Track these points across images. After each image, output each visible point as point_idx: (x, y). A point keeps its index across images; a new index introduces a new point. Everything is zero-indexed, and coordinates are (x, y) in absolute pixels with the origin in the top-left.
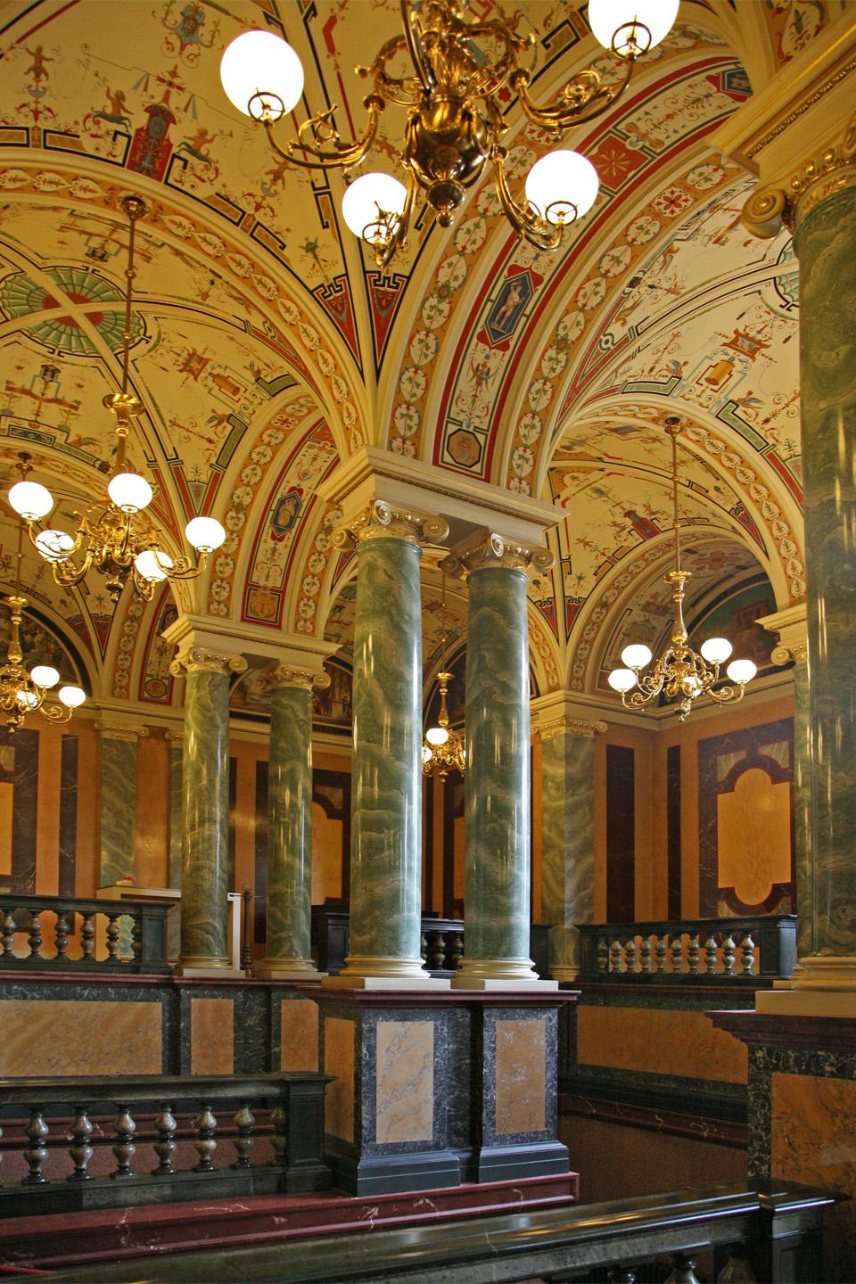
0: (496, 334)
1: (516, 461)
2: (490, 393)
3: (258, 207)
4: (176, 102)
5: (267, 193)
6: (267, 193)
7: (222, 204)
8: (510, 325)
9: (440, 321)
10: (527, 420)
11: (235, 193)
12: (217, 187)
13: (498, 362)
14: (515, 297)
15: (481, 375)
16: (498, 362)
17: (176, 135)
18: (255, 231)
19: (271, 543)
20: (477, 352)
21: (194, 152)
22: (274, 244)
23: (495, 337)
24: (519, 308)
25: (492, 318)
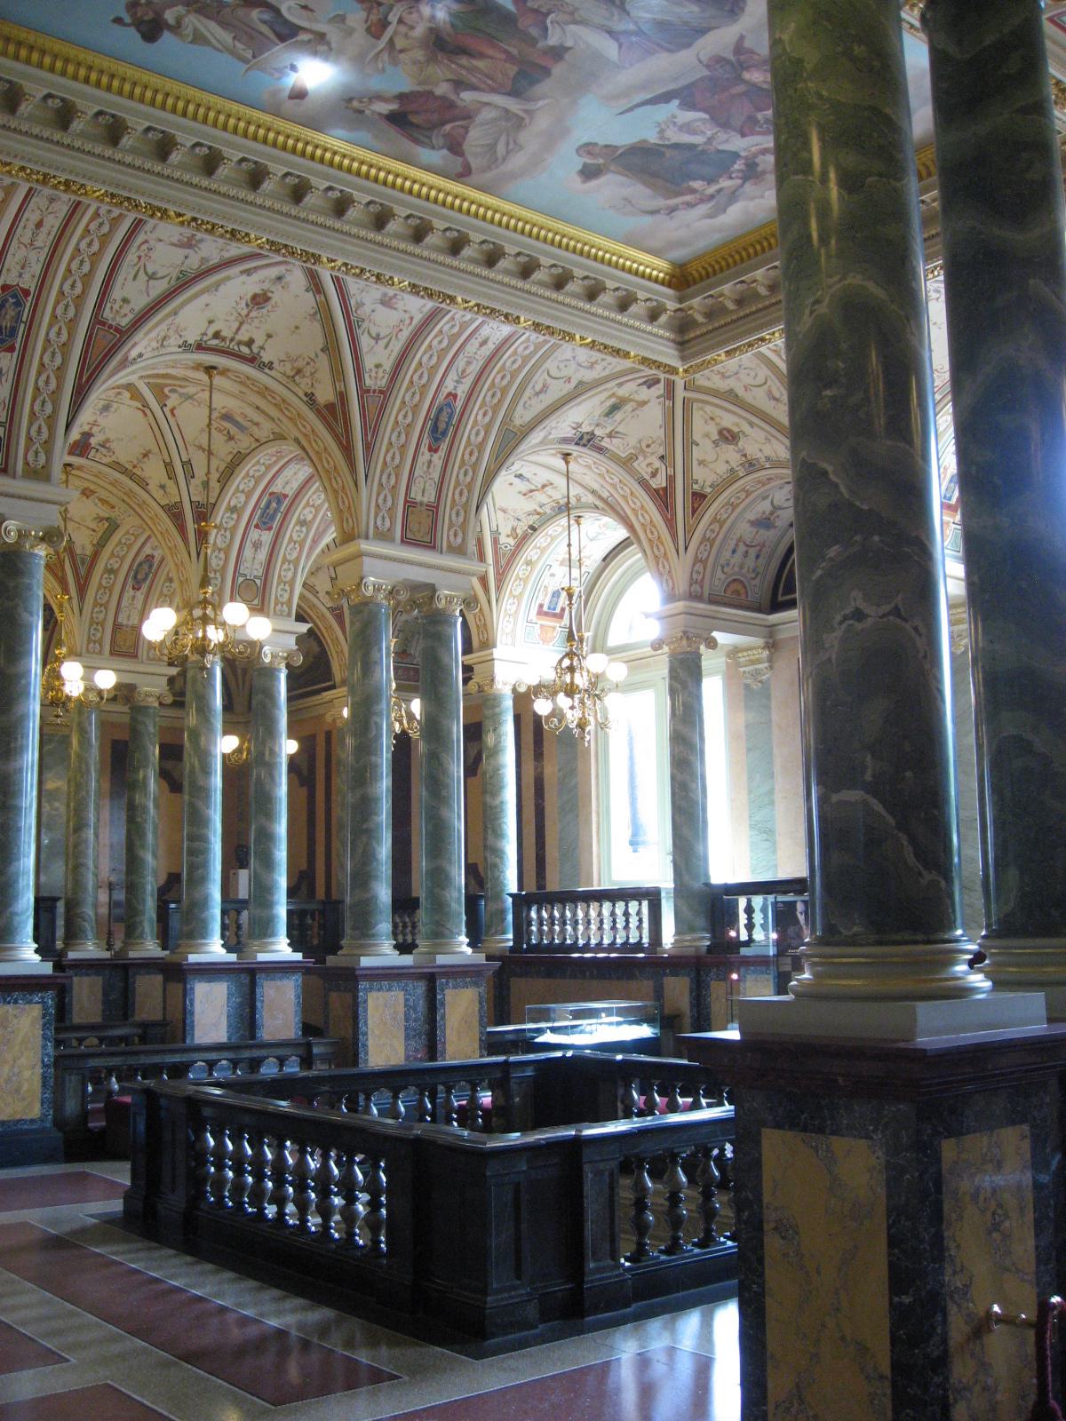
0: (265, 523)
1: (280, 592)
2: (262, 555)
3: (134, 467)
4: (95, 430)
5: (139, 461)
6: (139, 461)
7: (116, 466)
8: (273, 518)
9: (232, 523)
10: (285, 566)
11: (123, 460)
12: (114, 458)
13: (267, 537)
14: (274, 505)
15: (257, 546)
16: (267, 537)
17: (93, 441)
18: (132, 476)
19: (131, 592)
20: (254, 534)
21: (104, 447)
22: (143, 483)
23: (264, 524)
24: (276, 511)
25: (262, 515)
